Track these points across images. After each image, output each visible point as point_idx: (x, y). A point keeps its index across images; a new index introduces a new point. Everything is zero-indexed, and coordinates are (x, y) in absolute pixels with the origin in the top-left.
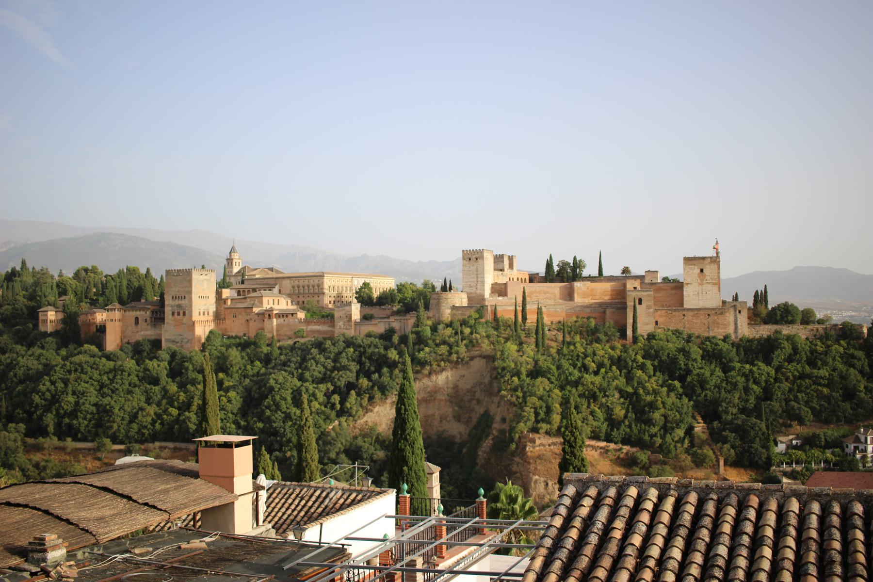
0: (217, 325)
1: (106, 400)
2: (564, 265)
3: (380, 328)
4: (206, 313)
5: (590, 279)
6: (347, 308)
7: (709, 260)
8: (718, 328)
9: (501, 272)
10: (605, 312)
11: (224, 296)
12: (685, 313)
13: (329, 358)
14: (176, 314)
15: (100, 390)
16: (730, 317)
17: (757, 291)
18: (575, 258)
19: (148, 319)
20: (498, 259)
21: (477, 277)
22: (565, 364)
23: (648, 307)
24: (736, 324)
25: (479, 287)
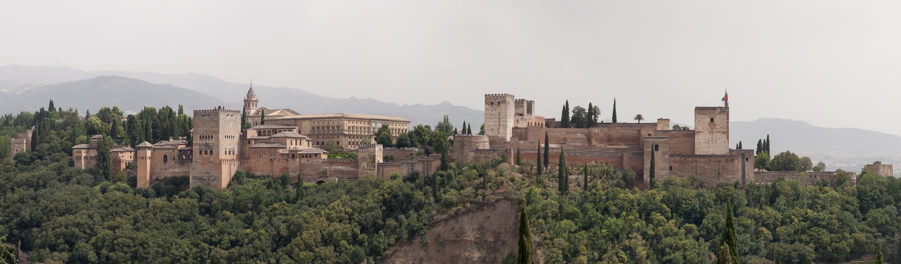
0: (241, 164)
1: (141, 235)
2: (579, 111)
3: (403, 171)
4: (232, 153)
5: (603, 124)
6: (371, 149)
7: (719, 110)
8: (727, 174)
9: (520, 117)
10: (622, 158)
11: (249, 137)
12: (698, 159)
13: (356, 199)
14: (203, 153)
15: (134, 224)
16: (738, 164)
17: (760, 141)
18: (590, 105)
19: (176, 157)
20: (519, 103)
21: (499, 122)
22: (589, 206)
23: (664, 154)
24: (744, 171)
25: (501, 131)
